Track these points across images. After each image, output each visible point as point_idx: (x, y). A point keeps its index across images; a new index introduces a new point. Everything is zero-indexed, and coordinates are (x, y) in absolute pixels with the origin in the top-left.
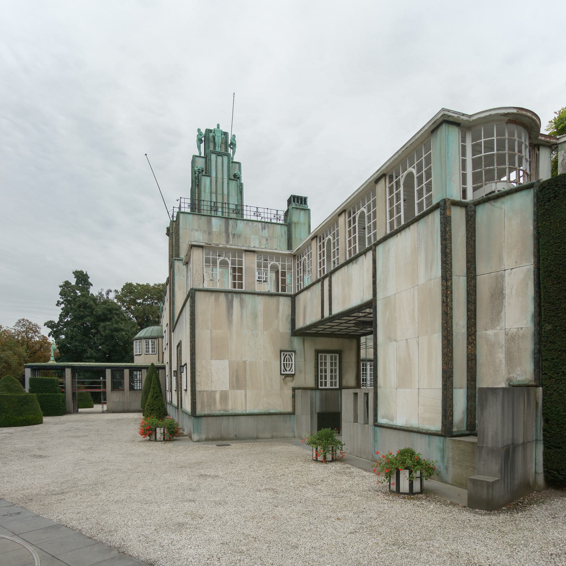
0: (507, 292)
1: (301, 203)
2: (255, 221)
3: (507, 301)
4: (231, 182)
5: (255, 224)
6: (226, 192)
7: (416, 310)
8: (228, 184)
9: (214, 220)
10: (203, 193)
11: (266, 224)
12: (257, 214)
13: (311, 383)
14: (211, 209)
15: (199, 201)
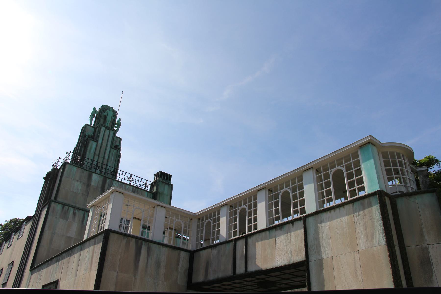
1: (167, 179)
2: (128, 184)
4: (112, 150)
6: (106, 157)
7: (359, 271)
8: (110, 151)
10: (88, 153)
11: (136, 189)
12: (130, 179)
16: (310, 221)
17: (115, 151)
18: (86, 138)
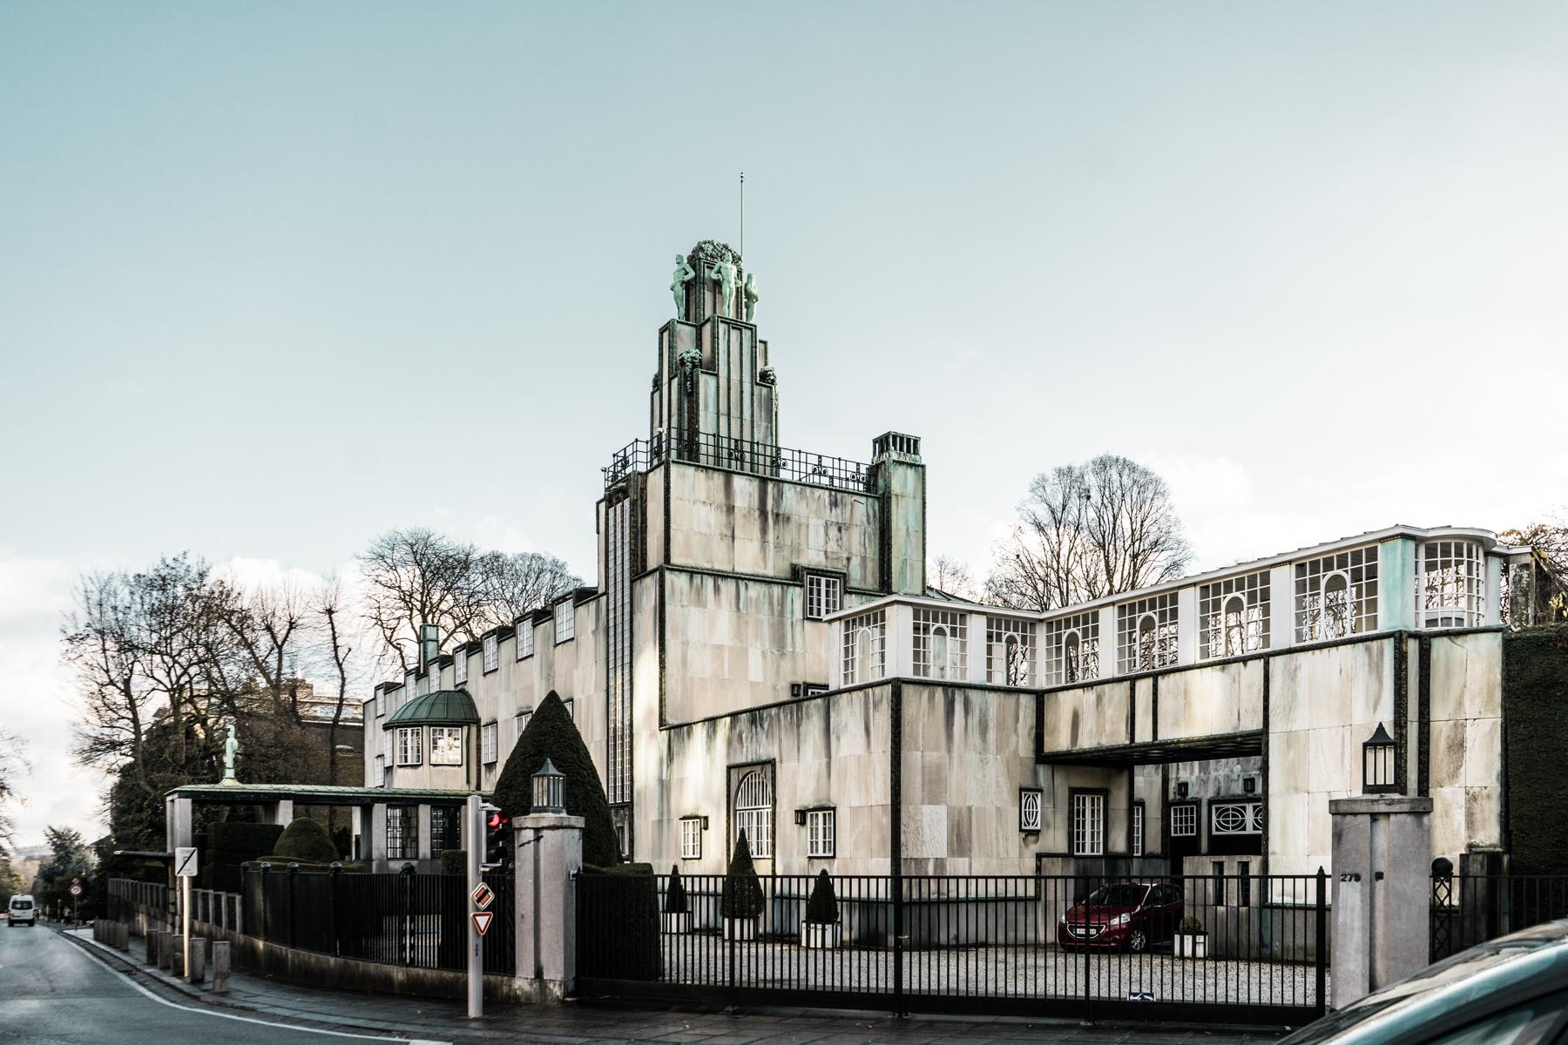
0: (1468, 744)
3: (1468, 755)
5: (818, 492)
7: (1347, 756)
9: (738, 482)
10: (702, 413)
13: (1061, 846)
14: (730, 454)
15: (697, 432)
16: (1277, 664)
17: (765, 391)
18: (688, 370)
